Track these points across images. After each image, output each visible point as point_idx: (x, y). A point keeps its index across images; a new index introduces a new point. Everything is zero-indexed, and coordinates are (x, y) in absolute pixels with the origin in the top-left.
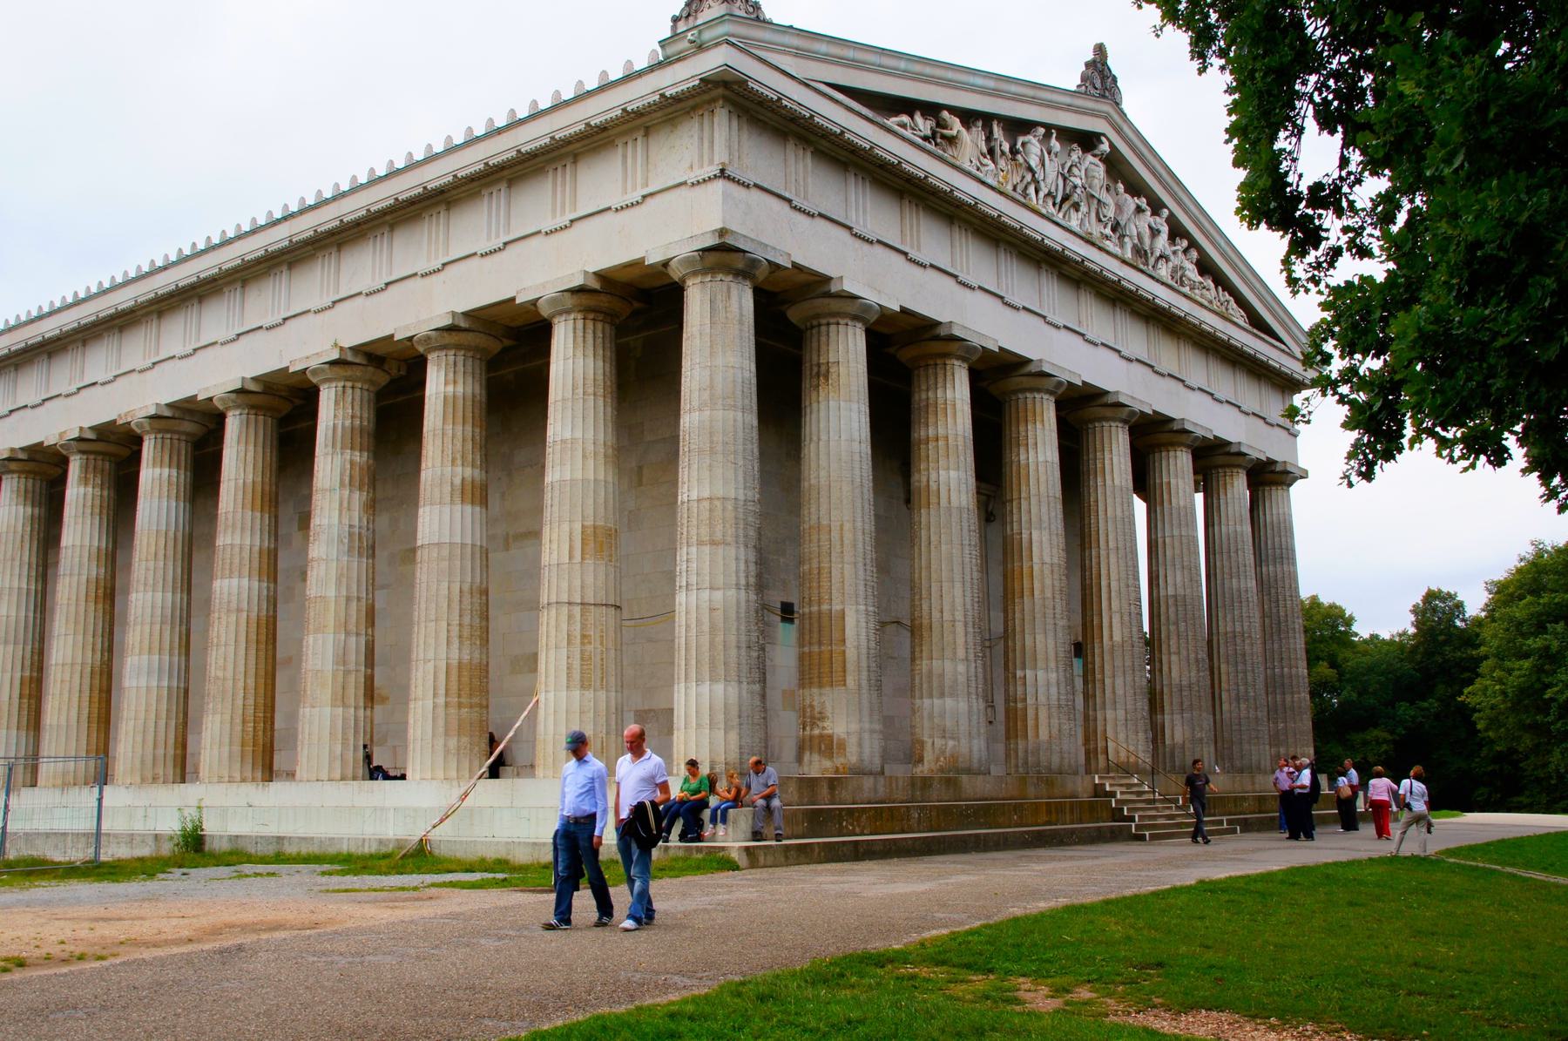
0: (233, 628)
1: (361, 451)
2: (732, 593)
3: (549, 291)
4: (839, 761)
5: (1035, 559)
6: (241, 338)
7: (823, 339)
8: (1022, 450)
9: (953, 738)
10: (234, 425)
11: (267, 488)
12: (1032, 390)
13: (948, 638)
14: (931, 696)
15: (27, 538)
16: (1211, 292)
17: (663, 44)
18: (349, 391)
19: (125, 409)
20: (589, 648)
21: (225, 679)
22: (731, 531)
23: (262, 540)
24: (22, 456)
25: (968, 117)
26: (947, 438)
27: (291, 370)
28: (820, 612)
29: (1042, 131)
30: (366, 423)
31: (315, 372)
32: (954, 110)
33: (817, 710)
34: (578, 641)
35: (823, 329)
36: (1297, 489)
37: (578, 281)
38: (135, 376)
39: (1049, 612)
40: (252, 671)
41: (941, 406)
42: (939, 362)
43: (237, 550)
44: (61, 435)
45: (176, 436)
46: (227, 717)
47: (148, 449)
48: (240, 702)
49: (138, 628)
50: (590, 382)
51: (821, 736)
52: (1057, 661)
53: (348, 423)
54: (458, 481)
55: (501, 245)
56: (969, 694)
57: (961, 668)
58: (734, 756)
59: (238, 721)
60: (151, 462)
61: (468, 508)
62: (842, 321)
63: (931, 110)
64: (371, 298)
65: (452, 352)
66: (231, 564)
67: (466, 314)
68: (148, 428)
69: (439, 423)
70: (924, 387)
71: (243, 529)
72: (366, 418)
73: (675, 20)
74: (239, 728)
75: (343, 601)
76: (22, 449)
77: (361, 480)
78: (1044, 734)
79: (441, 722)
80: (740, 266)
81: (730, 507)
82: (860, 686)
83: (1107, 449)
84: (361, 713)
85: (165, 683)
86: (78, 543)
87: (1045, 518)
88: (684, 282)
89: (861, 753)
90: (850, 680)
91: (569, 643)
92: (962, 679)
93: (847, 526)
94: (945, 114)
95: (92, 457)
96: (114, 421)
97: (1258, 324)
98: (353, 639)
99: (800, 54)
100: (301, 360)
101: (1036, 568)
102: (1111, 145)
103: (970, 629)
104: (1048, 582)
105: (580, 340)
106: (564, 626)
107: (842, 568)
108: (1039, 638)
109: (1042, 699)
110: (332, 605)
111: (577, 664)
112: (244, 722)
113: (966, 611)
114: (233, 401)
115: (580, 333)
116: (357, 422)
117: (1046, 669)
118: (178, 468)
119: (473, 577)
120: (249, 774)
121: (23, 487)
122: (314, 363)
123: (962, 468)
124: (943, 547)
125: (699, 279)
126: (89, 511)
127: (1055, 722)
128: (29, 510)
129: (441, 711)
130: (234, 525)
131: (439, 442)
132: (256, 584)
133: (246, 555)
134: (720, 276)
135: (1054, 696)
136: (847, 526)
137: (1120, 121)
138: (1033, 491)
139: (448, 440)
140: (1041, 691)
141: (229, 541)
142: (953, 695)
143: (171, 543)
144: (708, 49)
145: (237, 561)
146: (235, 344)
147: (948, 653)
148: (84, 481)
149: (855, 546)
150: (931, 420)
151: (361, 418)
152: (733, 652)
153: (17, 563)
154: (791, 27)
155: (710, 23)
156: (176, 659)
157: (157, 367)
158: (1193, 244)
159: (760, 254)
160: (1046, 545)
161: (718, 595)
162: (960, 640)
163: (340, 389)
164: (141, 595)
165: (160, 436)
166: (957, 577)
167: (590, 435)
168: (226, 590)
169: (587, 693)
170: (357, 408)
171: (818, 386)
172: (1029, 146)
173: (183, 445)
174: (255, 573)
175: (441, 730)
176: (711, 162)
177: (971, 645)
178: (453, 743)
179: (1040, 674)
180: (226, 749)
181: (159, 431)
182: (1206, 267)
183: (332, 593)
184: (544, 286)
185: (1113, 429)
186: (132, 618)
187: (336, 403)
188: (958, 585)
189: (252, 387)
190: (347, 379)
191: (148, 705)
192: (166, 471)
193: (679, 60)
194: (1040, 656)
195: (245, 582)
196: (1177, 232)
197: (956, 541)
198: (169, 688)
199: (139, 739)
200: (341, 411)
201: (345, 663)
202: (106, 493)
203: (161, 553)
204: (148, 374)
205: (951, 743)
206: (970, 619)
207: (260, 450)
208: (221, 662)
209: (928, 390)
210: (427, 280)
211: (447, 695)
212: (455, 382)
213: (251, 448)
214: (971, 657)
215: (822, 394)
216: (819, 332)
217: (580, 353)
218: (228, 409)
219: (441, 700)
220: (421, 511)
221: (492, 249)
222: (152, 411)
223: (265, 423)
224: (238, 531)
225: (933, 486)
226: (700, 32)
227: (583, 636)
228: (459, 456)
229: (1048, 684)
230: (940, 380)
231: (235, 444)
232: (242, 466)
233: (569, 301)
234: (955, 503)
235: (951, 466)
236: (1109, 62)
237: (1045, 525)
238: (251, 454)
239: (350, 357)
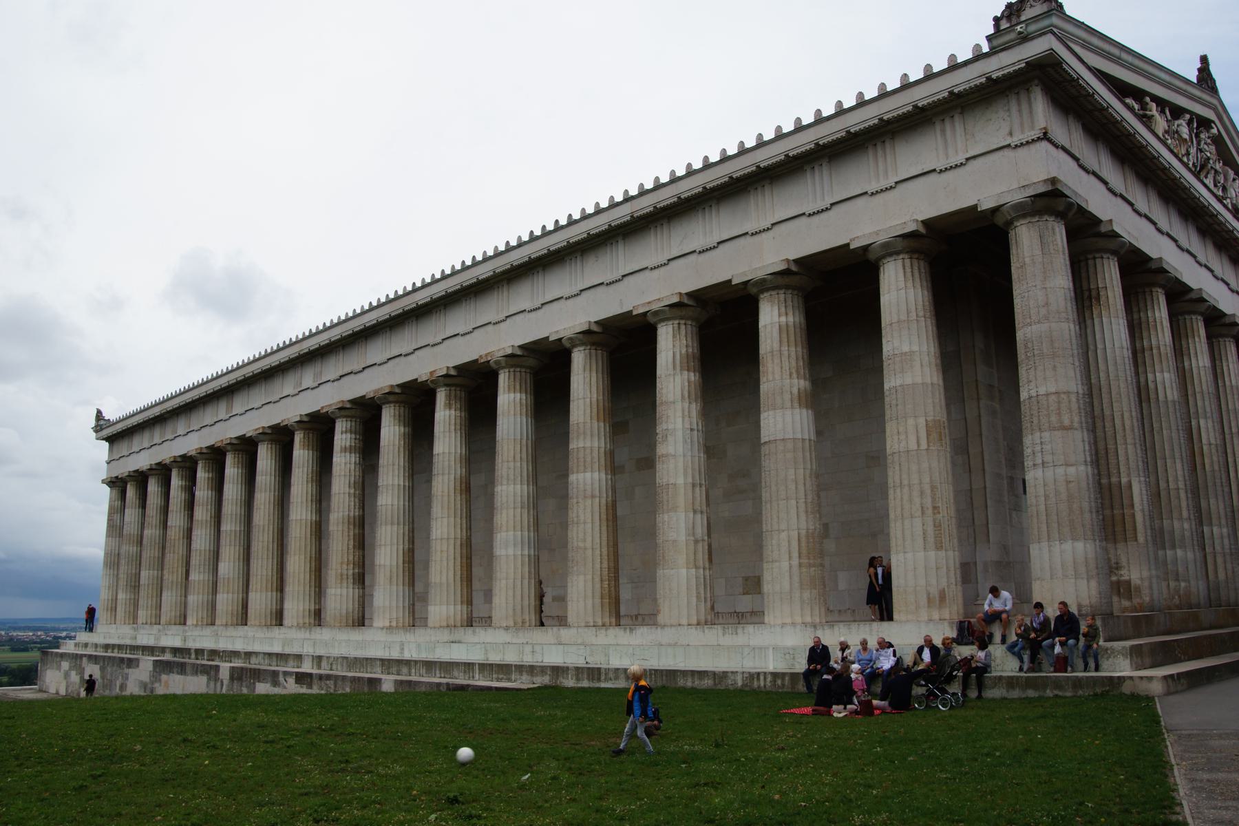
0: (589, 510)
1: (694, 372)
2: (1082, 468)
4: (1136, 601)
5: (1204, 441)
6: (583, 293)
7: (1091, 270)
8: (1186, 358)
9: (1185, 581)
10: (579, 358)
11: (606, 404)
12: (1190, 313)
13: (1174, 502)
14: (1173, 547)
15: (402, 449)
17: (989, 38)
18: (683, 327)
19: (483, 352)
20: (939, 516)
21: (585, 549)
22: (1076, 419)
23: (605, 443)
24: (397, 390)
26: (1159, 348)
27: (635, 313)
28: (1110, 484)
29: (1188, 116)
30: (696, 351)
31: (656, 313)
33: (1113, 561)
34: (930, 512)
35: (1091, 262)
37: (911, 227)
38: (490, 327)
39: (1218, 481)
40: (605, 543)
41: (1151, 324)
42: (1147, 290)
43: (588, 451)
44: (432, 373)
45: (523, 370)
46: (589, 577)
47: (503, 379)
48: (598, 566)
49: (504, 512)
50: (920, 307)
51: (1118, 582)
52: (1227, 519)
53: (684, 351)
54: (795, 391)
55: (829, 206)
56: (1193, 545)
57: (1186, 526)
58: (1094, 600)
59: (597, 579)
60: (507, 389)
61: (804, 411)
62: (1105, 256)
63: (1139, 94)
64: (703, 255)
65: (782, 292)
66: (585, 462)
67: (796, 261)
68: (503, 365)
69: (776, 346)
70: (1135, 309)
71: (592, 436)
72: (694, 348)
73: (997, 20)
74: (598, 586)
75: (690, 488)
76: (398, 385)
77: (696, 394)
78: (1222, 576)
79: (796, 579)
80: (1061, 208)
81: (1074, 399)
82: (1147, 541)
83: (1224, 358)
84: (707, 572)
85: (526, 552)
86: (447, 451)
87: (1208, 409)
88: (1009, 223)
89: (1151, 595)
90: (1141, 539)
91: (923, 513)
92: (1187, 534)
93: (1126, 415)
95: (453, 388)
96: (476, 360)
98: (699, 516)
99: (1086, 46)
100: (643, 305)
101: (1205, 448)
103: (1190, 495)
104: (1215, 458)
105: (909, 274)
106: (917, 500)
107: (1126, 448)
108: (1212, 501)
109: (1218, 548)
110: (682, 491)
111: (930, 530)
112: (602, 581)
113: (1185, 481)
114: (580, 340)
115: (908, 270)
116: (690, 350)
117: (1220, 526)
118: (526, 393)
119: (811, 464)
120: (607, 620)
121: (397, 413)
122: (655, 307)
123: (1172, 371)
124: (1165, 432)
126: (453, 428)
127: (1229, 566)
128: (402, 429)
129: (796, 570)
130: (584, 433)
131: (777, 361)
132: (603, 476)
133: (595, 454)
134: (1046, 217)
135: (1227, 547)
136: (1126, 415)
138: (1197, 390)
139: (785, 359)
140: (1217, 542)
141: (581, 445)
142: (1183, 547)
143: (524, 449)
144: (1033, 38)
145: (589, 459)
146: (579, 298)
147: (1175, 515)
148: (449, 406)
149: (1133, 430)
150: (1145, 334)
151: (693, 347)
152: (1087, 516)
153: (396, 467)
154: (1083, 23)
155: (1036, 19)
156: (532, 534)
157: (508, 320)
159: (1074, 199)
160: (1211, 430)
161: (1072, 470)
162: (1184, 504)
163: (676, 326)
164: (504, 487)
165: (512, 370)
166: (1177, 455)
167: (925, 348)
168: (589, 481)
169: (940, 553)
170: (689, 339)
171: (1092, 306)
173: (528, 375)
174: (603, 468)
175: (796, 585)
176: (1033, 128)
177: (1191, 507)
178: (807, 595)
179: (1215, 529)
180: (590, 602)
181: (512, 366)
183: (681, 481)
184: (877, 233)
185: (1227, 343)
186: (499, 504)
187: (674, 336)
188: (1178, 461)
189: (595, 328)
190: (682, 318)
191: (515, 568)
192: (518, 395)
194: (1214, 516)
195: (596, 475)
197: (1174, 428)
198: (529, 556)
199: (511, 593)
200: (678, 342)
201: (694, 534)
202: (463, 414)
203: (518, 456)
204: (502, 325)
205: (1183, 584)
206: (1188, 487)
207: (600, 375)
208: (581, 536)
209: (1139, 311)
210: (756, 238)
211: (800, 557)
212: (787, 314)
213: (594, 374)
214: (1192, 517)
215: (1095, 313)
216: (1087, 265)
217: (910, 284)
218: (574, 346)
219: (795, 562)
220: (763, 416)
221: (820, 209)
222: (509, 351)
223: (602, 354)
224: (589, 437)
225: (1151, 385)
226: (1027, 26)
227: (935, 508)
228: (794, 371)
229: (1222, 537)
230: (1149, 303)
231: (581, 371)
232: (588, 388)
234: (1170, 397)
235: (1165, 369)
236: (1211, 68)
237: (1209, 415)
238: (594, 379)
239: (686, 301)
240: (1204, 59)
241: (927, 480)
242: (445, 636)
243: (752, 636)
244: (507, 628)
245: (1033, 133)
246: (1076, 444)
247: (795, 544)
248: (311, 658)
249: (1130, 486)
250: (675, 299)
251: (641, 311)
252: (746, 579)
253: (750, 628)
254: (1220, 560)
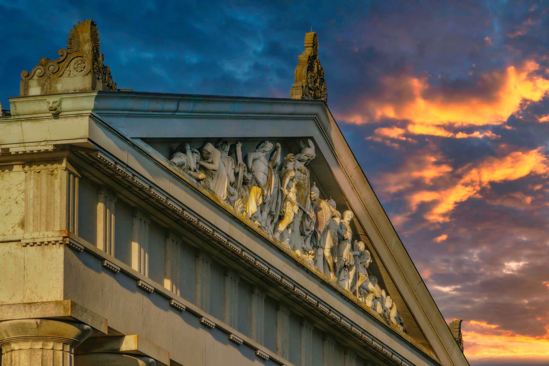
29: (269, 146)
32: (218, 142)
94: (210, 147)
102: (317, 149)
125: (26, 346)
172: (258, 162)
193: (28, 120)
245: (50, 234)
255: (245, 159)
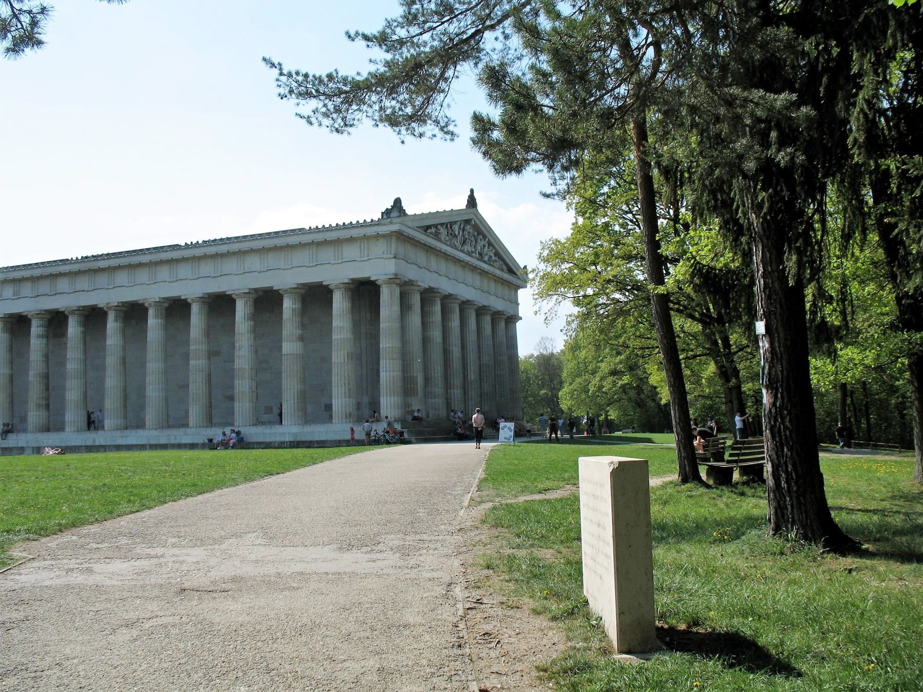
3: (336, 282)
16: (499, 263)
25: (442, 224)
29: (459, 223)
31: (237, 295)
36: (519, 325)
37: (346, 281)
44: (107, 304)
63: (436, 226)
90: (419, 395)
94: (439, 226)
97: (511, 271)
106: (343, 380)
111: (347, 391)
122: (237, 292)
137: (478, 215)
158: (494, 247)
161: (395, 373)
178: (300, 414)
182: (497, 254)
183: (247, 367)
196: (490, 244)
219: (296, 401)
233: (342, 286)
240: (472, 191)
241: (346, 373)
242: (118, 433)
243: (278, 429)
244: (156, 429)
246: (397, 364)
247: (296, 394)
248: (31, 450)
249: (417, 377)
250: (247, 291)
251: (230, 293)
252: (266, 407)
253: (278, 426)
254: (456, 403)
255: (451, 228)
